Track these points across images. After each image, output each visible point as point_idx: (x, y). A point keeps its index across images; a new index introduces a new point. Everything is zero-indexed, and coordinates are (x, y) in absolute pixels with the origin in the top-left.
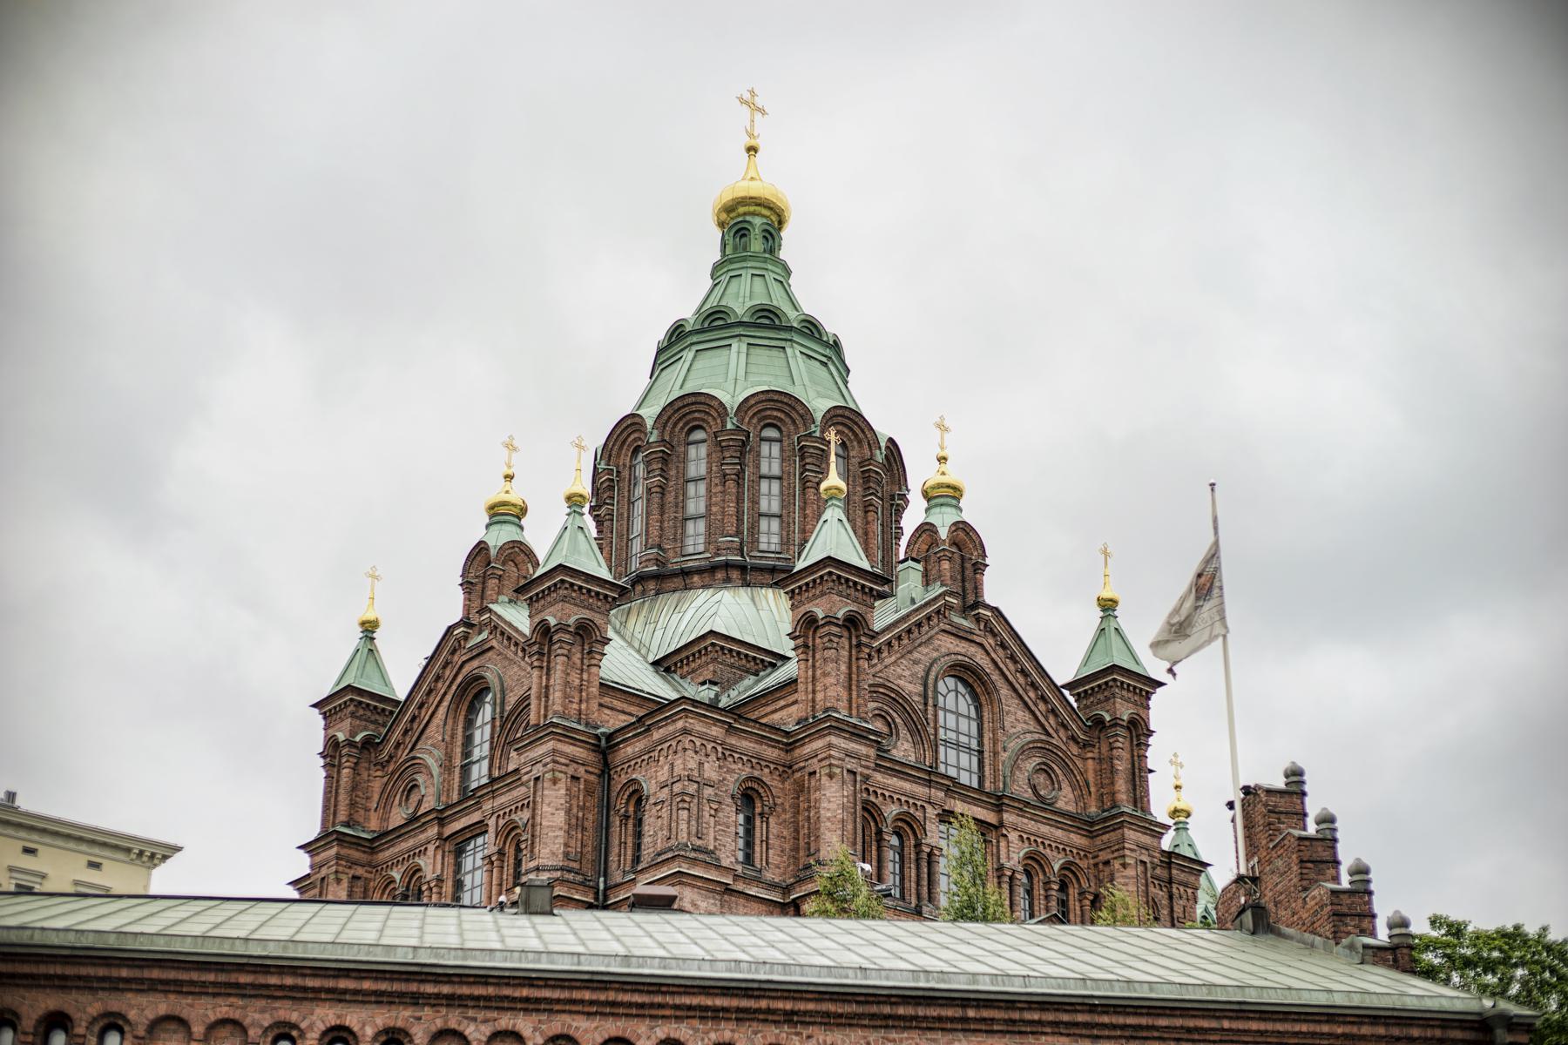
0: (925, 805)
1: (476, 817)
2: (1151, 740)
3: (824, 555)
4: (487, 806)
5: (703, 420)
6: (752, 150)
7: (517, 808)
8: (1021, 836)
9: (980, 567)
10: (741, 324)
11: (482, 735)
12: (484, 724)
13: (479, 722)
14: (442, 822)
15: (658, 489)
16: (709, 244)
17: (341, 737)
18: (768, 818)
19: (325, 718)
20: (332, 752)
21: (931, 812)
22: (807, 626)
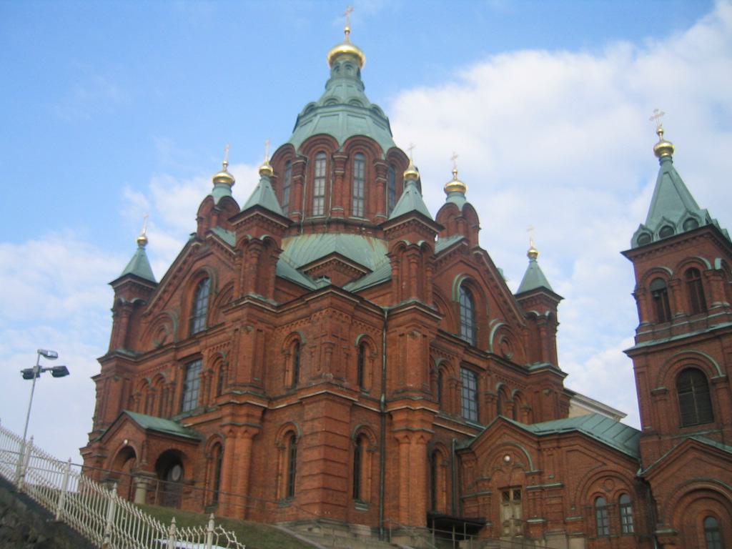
0: (455, 358)
1: (194, 350)
2: (558, 328)
3: (412, 209)
4: (203, 343)
7: (221, 346)
8: (496, 376)
9: (477, 229)
11: (203, 304)
12: (204, 298)
13: (201, 296)
14: (177, 349)
16: (326, 71)
17: (123, 300)
18: (373, 361)
19: (116, 290)
20: (118, 309)
21: (457, 361)
22: (398, 252)
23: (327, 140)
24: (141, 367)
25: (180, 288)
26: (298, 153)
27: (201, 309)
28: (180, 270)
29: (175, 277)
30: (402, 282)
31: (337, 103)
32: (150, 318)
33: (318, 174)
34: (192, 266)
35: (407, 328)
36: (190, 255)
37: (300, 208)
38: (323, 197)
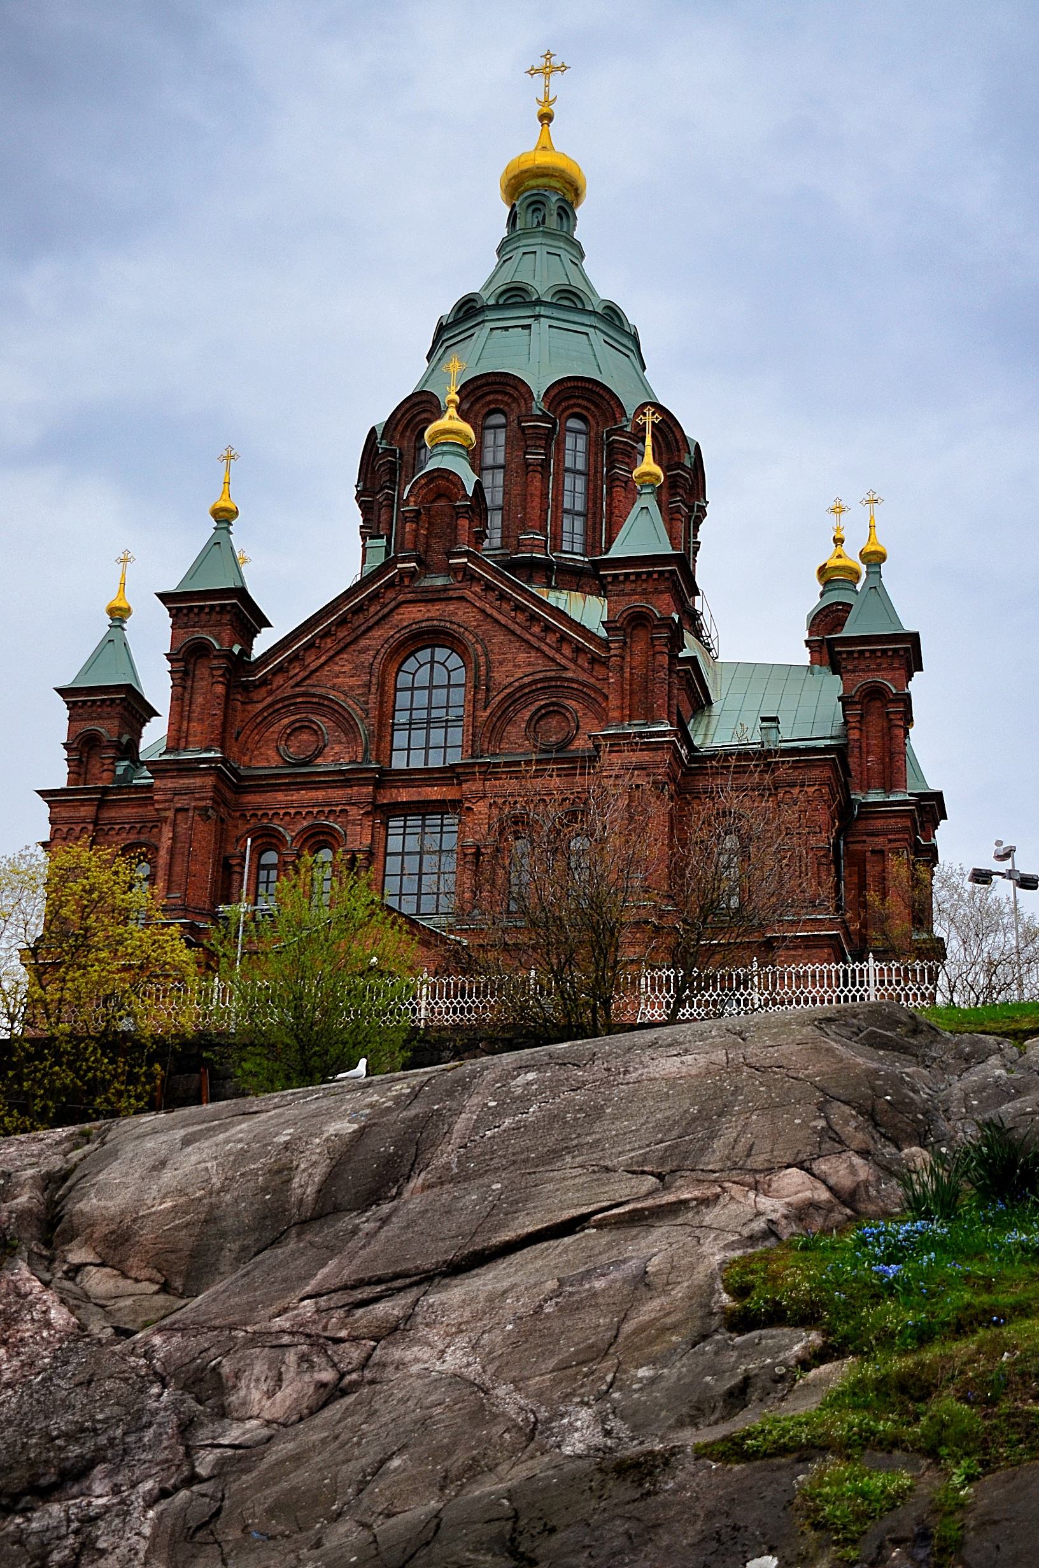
5: (588, 409)
6: (546, 118)
10: (593, 313)
14: (379, 785)
15: (539, 469)
23: (598, 394)
24: (250, 798)
25: (353, 647)
26: (538, 406)
27: (429, 708)
28: (358, 609)
29: (342, 622)
30: (868, 753)
31: (580, 306)
32: (263, 692)
33: (568, 463)
34: (392, 611)
35: (890, 841)
36: (390, 585)
37: (543, 529)
38: (579, 514)
